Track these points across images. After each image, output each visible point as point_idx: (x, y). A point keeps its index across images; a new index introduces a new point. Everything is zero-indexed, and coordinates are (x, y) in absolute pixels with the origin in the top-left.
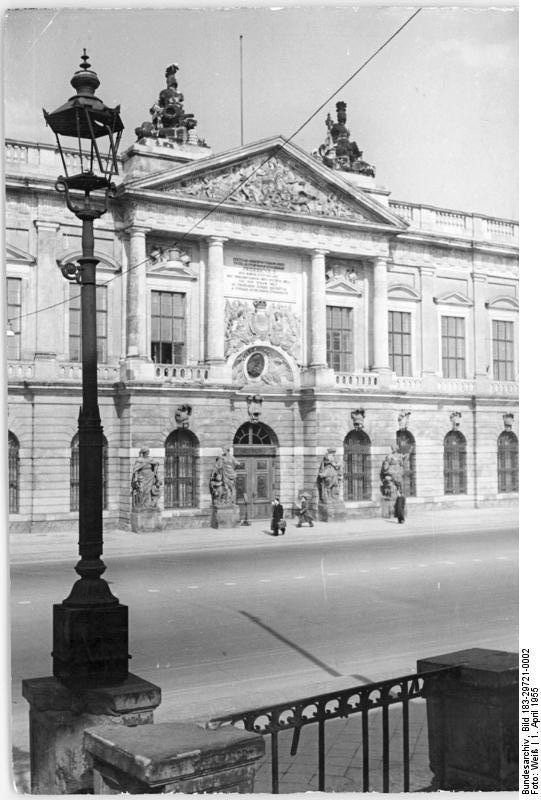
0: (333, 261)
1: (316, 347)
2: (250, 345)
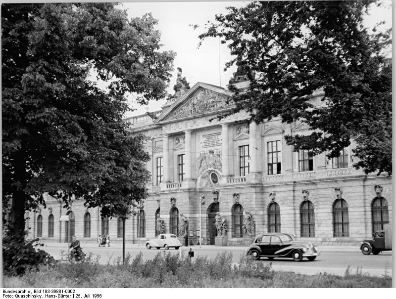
1: (269, 159)
2: (207, 170)
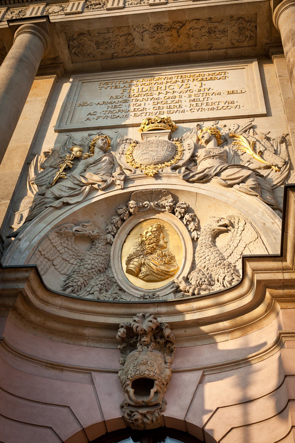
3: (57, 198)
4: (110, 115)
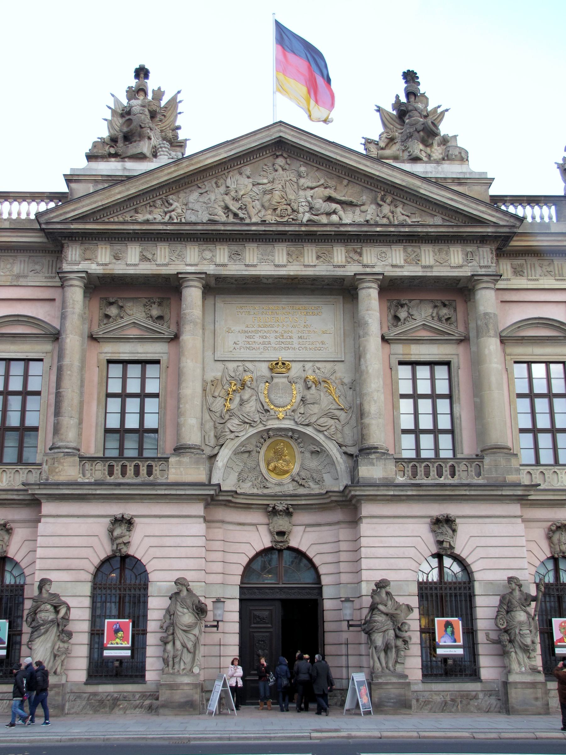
0: (394, 289)
2: (261, 428)
3: (232, 432)
4: (248, 346)
